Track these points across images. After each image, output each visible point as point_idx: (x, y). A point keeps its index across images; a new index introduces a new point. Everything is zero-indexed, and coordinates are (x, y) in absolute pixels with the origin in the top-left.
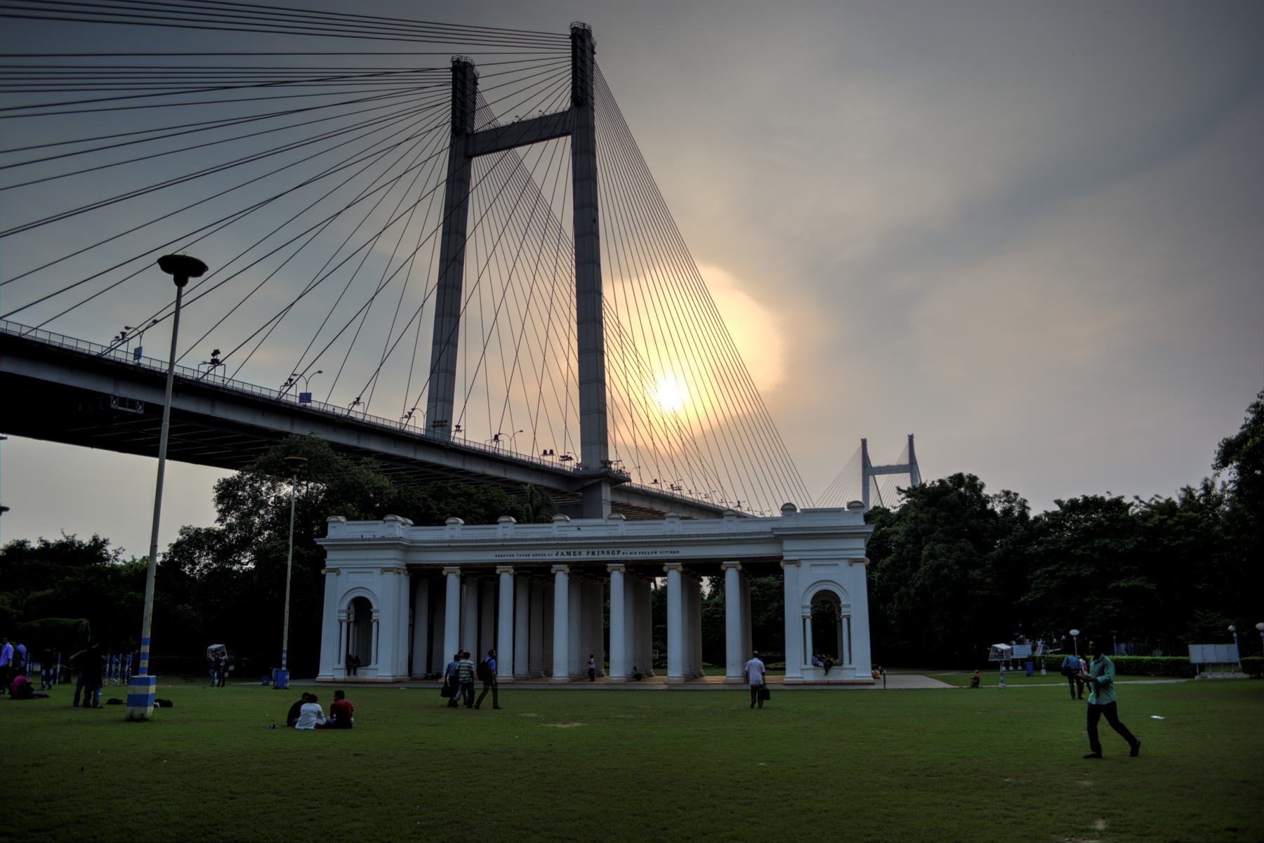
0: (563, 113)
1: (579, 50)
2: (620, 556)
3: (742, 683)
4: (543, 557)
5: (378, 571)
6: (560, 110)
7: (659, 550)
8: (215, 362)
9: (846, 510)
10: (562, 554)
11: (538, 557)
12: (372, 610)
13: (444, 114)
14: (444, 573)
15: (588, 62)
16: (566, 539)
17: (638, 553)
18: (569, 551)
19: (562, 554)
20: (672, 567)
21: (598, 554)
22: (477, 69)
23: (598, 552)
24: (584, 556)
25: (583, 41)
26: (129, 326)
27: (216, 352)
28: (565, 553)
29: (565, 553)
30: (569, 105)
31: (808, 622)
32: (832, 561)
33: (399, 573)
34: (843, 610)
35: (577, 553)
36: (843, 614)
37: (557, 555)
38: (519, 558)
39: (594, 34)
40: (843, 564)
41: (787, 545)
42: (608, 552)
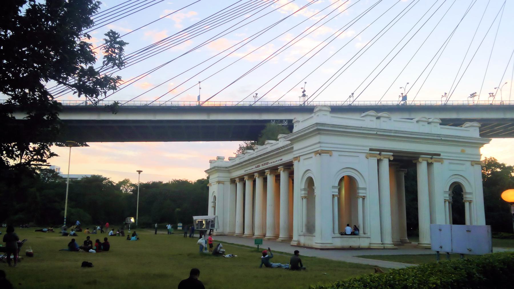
2: (270, 165)
5: (215, 183)
8: (304, 95)
24: (261, 168)
27: (304, 91)
31: (304, 200)
33: (223, 184)
41: (296, 146)
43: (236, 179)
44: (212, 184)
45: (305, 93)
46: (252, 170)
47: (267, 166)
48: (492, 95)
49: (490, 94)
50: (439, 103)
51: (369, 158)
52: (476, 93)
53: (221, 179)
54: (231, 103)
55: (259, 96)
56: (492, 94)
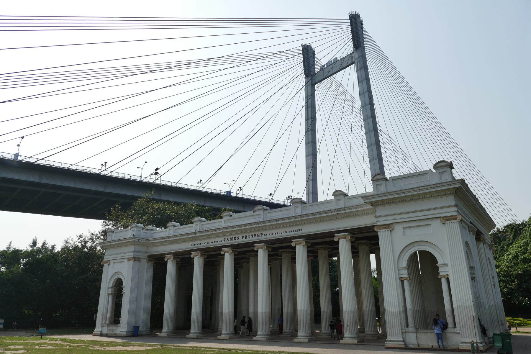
0: (351, 54)
1: (354, 24)
3: (356, 344)
4: (217, 243)
5: (126, 260)
6: (349, 53)
7: (287, 230)
8: (157, 173)
9: (434, 171)
10: (228, 239)
11: (214, 244)
12: (122, 286)
13: (301, 68)
14: (165, 260)
15: (359, 29)
16: (231, 227)
17: (274, 234)
18: (231, 237)
19: (228, 239)
20: (297, 242)
21: (249, 238)
22: (313, 47)
23: (249, 236)
24: (241, 240)
25: (356, 19)
26: (139, 167)
27: (157, 169)
28: (229, 239)
29: (229, 239)
30: (353, 50)
32: (425, 222)
33: (139, 261)
34: (441, 269)
35: (236, 238)
36: (441, 274)
37: (224, 241)
38: (204, 245)
39: (361, 16)
40: (436, 224)
42: (255, 235)
43: (165, 256)
44: (112, 262)
45: (158, 171)
46: (215, 243)
47: (257, 238)
50: (264, 200)
51: (471, 232)
53: (138, 255)
54: (83, 168)
55: (108, 165)
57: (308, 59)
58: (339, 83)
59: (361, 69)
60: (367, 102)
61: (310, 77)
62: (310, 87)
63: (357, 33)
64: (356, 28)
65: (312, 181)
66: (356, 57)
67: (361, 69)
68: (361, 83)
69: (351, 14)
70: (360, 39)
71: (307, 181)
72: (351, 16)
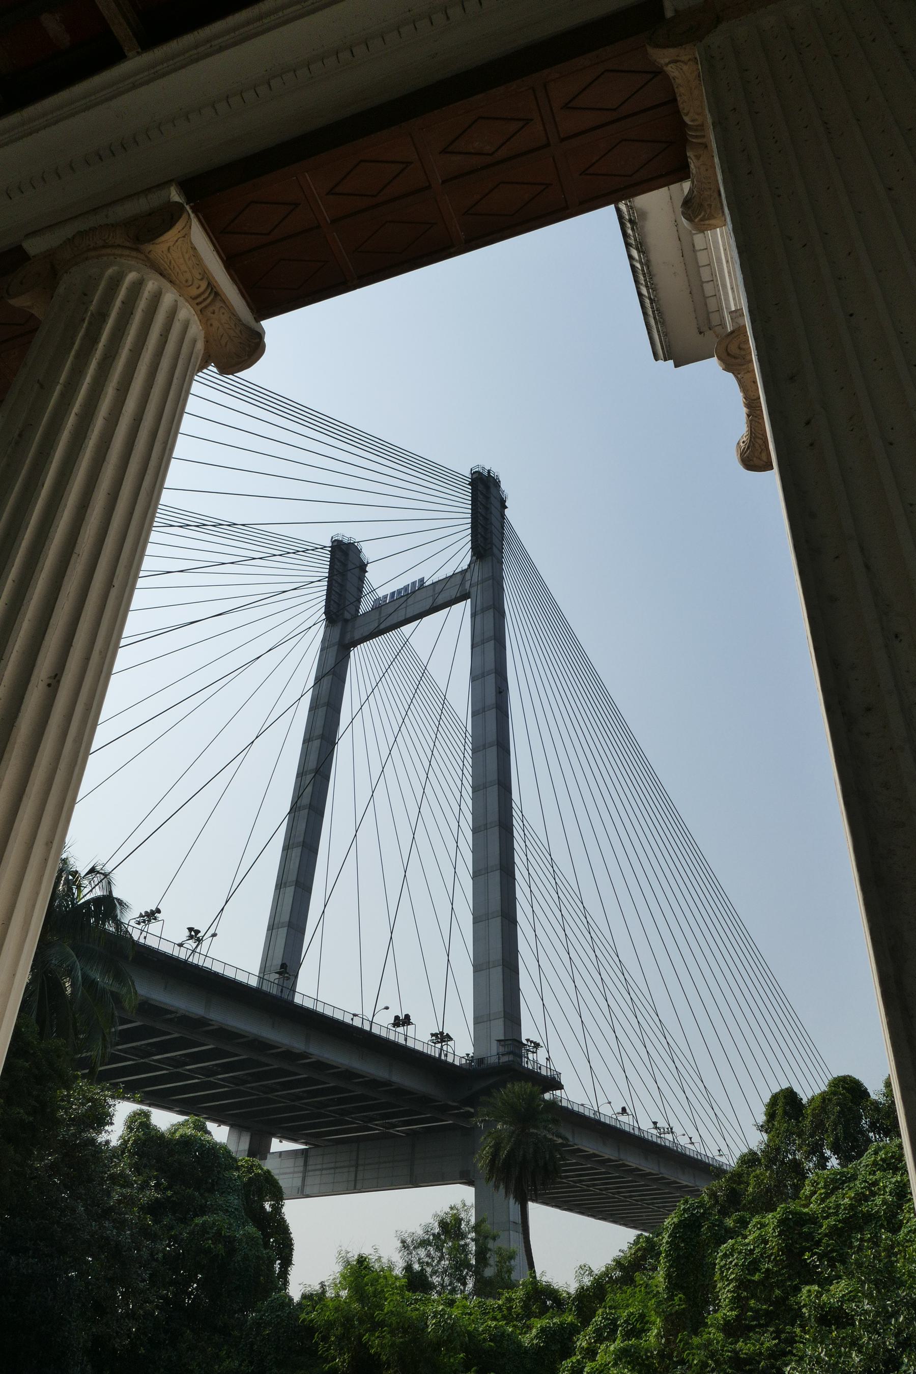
0: (464, 572)
22: (368, 552)
25: (488, 488)
39: (503, 486)
48: (194, 934)
49: (190, 929)
52: (158, 911)
56: (197, 932)
57: (343, 575)
58: (422, 665)
59: (483, 611)
60: (491, 699)
61: (340, 625)
62: (333, 651)
63: (486, 519)
64: (487, 509)
65: (286, 929)
66: (475, 579)
67: (483, 611)
68: (477, 649)
69: (476, 472)
70: (494, 537)
71: (271, 928)
72: (474, 476)
